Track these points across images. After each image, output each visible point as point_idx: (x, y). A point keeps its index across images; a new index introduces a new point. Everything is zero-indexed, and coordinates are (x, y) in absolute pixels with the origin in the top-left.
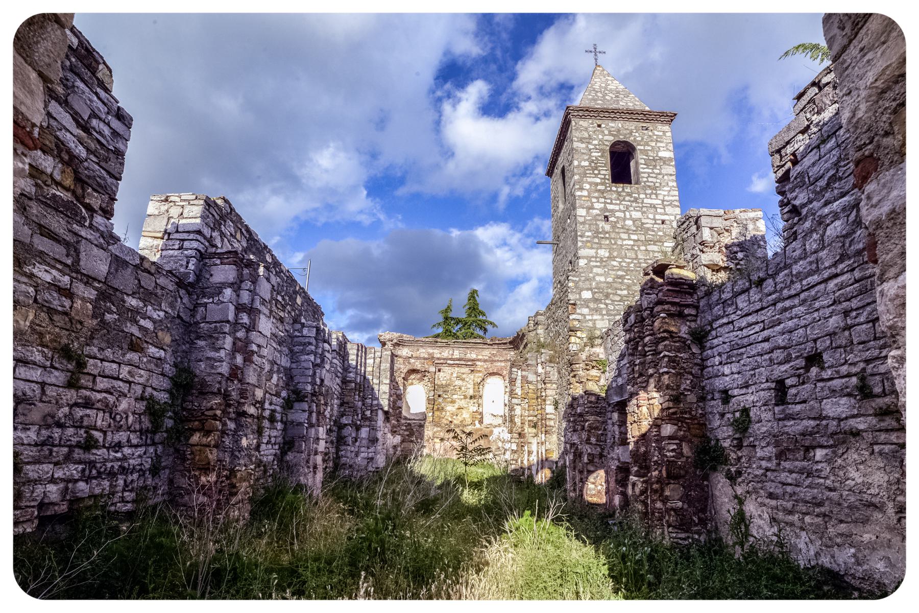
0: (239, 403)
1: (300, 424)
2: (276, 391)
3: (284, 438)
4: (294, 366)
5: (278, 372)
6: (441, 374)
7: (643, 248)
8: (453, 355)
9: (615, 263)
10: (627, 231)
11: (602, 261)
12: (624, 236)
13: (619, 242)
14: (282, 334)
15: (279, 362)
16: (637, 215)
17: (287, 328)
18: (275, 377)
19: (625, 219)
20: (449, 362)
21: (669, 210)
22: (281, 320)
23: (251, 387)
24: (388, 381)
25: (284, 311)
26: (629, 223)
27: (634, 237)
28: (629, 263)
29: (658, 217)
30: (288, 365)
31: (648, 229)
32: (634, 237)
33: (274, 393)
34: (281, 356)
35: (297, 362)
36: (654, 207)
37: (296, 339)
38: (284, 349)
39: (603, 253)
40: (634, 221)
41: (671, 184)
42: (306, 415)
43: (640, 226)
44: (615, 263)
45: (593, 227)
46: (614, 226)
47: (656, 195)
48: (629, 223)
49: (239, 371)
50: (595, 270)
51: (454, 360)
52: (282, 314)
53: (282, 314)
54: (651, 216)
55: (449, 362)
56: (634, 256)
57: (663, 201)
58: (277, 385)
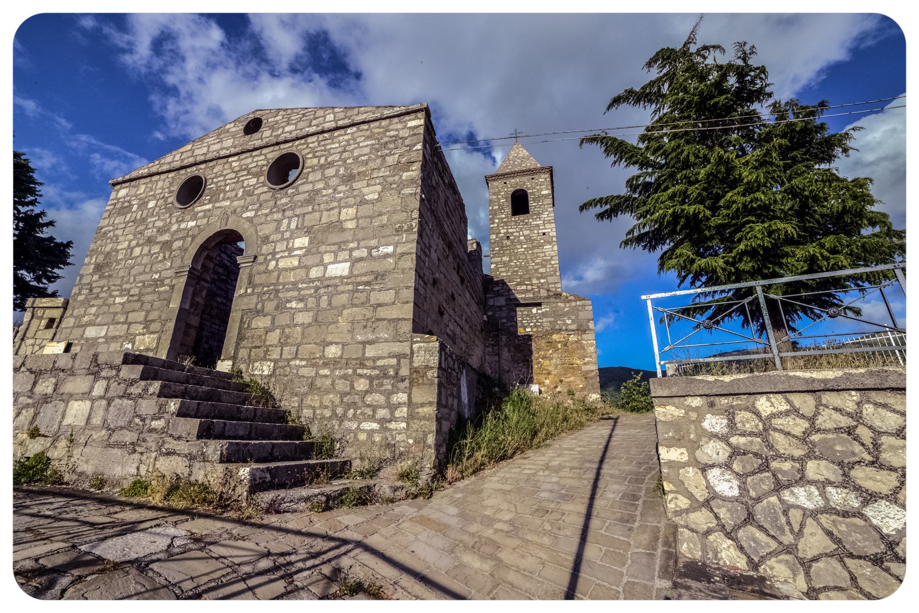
7: (530, 252)
9: (512, 264)
10: (521, 243)
11: (504, 263)
12: (519, 247)
13: (516, 251)
16: (526, 232)
19: (520, 236)
21: (547, 226)
26: (522, 238)
27: (525, 246)
28: (521, 263)
29: (540, 231)
31: (534, 240)
32: (525, 246)
36: (538, 226)
39: (506, 259)
40: (525, 236)
41: (549, 210)
43: (528, 239)
44: (512, 264)
45: (500, 245)
46: (512, 242)
47: (540, 218)
48: (523, 238)
50: (500, 270)
54: (536, 232)
56: (524, 257)
57: (544, 221)
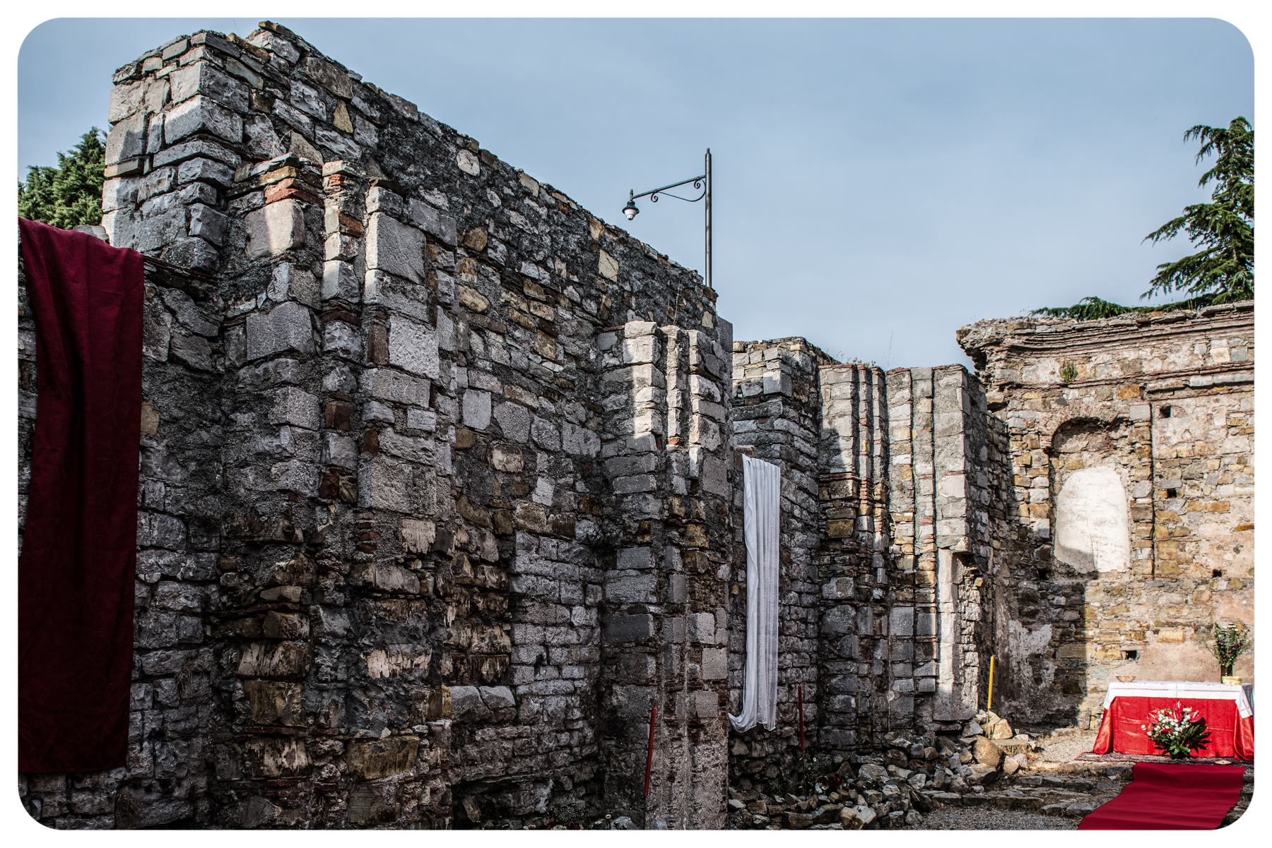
0: (353, 562)
1: (638, 608)
2: (555, 525)
3: (601, 648)
4: (609, 450)
5: (554, 472)
6: (1173, 423)
8: (1207, 355)
14: (558, 368)
15: (553, 444)
17: (573, 349)
18: (544, 490)
20: (1194, 381)
22: (548, 329)
23: (381, 517)
24: (960, 465)
25: (554, 304)
30: (593, 449)
33: (548, 529)
34: (559, 427)
35: (617, 437)
37: (607, 377)
38: (568, 408)
42: (649, 582)
49: (344, 480)
51: (1212, 372)
52: (547, 313)
53: (547, 313)
55: (1195, 381)
58: (556, 508)
